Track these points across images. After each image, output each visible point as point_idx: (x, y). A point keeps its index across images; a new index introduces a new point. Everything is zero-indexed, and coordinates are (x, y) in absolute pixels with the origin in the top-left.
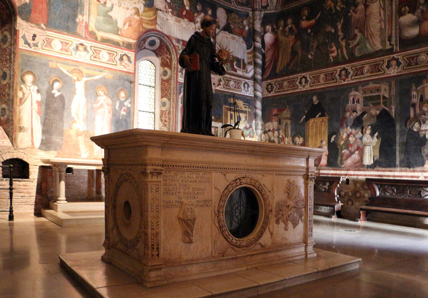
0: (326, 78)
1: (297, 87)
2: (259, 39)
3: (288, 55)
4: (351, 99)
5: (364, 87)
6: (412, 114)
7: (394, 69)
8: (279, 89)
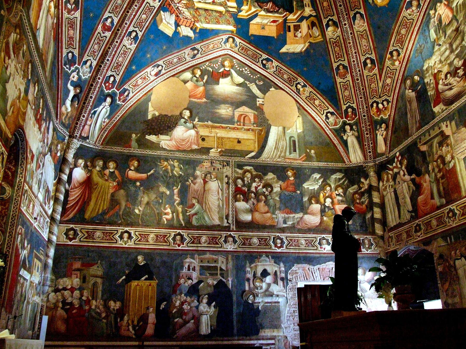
0: (157, 239)
1: (115, 241)
2: (67, 171)
3: (106, 202)
4: (186, 266)
5: (202, 256)
6: (247, 288)
7: (231, 245)
8: (86, 238)
